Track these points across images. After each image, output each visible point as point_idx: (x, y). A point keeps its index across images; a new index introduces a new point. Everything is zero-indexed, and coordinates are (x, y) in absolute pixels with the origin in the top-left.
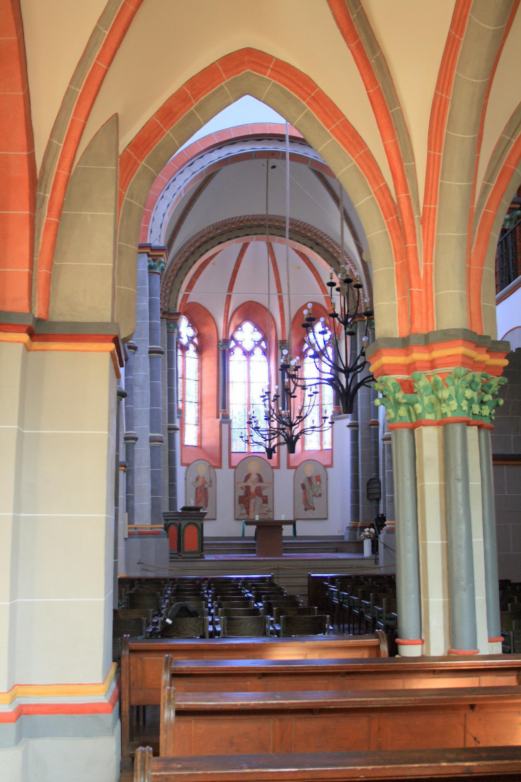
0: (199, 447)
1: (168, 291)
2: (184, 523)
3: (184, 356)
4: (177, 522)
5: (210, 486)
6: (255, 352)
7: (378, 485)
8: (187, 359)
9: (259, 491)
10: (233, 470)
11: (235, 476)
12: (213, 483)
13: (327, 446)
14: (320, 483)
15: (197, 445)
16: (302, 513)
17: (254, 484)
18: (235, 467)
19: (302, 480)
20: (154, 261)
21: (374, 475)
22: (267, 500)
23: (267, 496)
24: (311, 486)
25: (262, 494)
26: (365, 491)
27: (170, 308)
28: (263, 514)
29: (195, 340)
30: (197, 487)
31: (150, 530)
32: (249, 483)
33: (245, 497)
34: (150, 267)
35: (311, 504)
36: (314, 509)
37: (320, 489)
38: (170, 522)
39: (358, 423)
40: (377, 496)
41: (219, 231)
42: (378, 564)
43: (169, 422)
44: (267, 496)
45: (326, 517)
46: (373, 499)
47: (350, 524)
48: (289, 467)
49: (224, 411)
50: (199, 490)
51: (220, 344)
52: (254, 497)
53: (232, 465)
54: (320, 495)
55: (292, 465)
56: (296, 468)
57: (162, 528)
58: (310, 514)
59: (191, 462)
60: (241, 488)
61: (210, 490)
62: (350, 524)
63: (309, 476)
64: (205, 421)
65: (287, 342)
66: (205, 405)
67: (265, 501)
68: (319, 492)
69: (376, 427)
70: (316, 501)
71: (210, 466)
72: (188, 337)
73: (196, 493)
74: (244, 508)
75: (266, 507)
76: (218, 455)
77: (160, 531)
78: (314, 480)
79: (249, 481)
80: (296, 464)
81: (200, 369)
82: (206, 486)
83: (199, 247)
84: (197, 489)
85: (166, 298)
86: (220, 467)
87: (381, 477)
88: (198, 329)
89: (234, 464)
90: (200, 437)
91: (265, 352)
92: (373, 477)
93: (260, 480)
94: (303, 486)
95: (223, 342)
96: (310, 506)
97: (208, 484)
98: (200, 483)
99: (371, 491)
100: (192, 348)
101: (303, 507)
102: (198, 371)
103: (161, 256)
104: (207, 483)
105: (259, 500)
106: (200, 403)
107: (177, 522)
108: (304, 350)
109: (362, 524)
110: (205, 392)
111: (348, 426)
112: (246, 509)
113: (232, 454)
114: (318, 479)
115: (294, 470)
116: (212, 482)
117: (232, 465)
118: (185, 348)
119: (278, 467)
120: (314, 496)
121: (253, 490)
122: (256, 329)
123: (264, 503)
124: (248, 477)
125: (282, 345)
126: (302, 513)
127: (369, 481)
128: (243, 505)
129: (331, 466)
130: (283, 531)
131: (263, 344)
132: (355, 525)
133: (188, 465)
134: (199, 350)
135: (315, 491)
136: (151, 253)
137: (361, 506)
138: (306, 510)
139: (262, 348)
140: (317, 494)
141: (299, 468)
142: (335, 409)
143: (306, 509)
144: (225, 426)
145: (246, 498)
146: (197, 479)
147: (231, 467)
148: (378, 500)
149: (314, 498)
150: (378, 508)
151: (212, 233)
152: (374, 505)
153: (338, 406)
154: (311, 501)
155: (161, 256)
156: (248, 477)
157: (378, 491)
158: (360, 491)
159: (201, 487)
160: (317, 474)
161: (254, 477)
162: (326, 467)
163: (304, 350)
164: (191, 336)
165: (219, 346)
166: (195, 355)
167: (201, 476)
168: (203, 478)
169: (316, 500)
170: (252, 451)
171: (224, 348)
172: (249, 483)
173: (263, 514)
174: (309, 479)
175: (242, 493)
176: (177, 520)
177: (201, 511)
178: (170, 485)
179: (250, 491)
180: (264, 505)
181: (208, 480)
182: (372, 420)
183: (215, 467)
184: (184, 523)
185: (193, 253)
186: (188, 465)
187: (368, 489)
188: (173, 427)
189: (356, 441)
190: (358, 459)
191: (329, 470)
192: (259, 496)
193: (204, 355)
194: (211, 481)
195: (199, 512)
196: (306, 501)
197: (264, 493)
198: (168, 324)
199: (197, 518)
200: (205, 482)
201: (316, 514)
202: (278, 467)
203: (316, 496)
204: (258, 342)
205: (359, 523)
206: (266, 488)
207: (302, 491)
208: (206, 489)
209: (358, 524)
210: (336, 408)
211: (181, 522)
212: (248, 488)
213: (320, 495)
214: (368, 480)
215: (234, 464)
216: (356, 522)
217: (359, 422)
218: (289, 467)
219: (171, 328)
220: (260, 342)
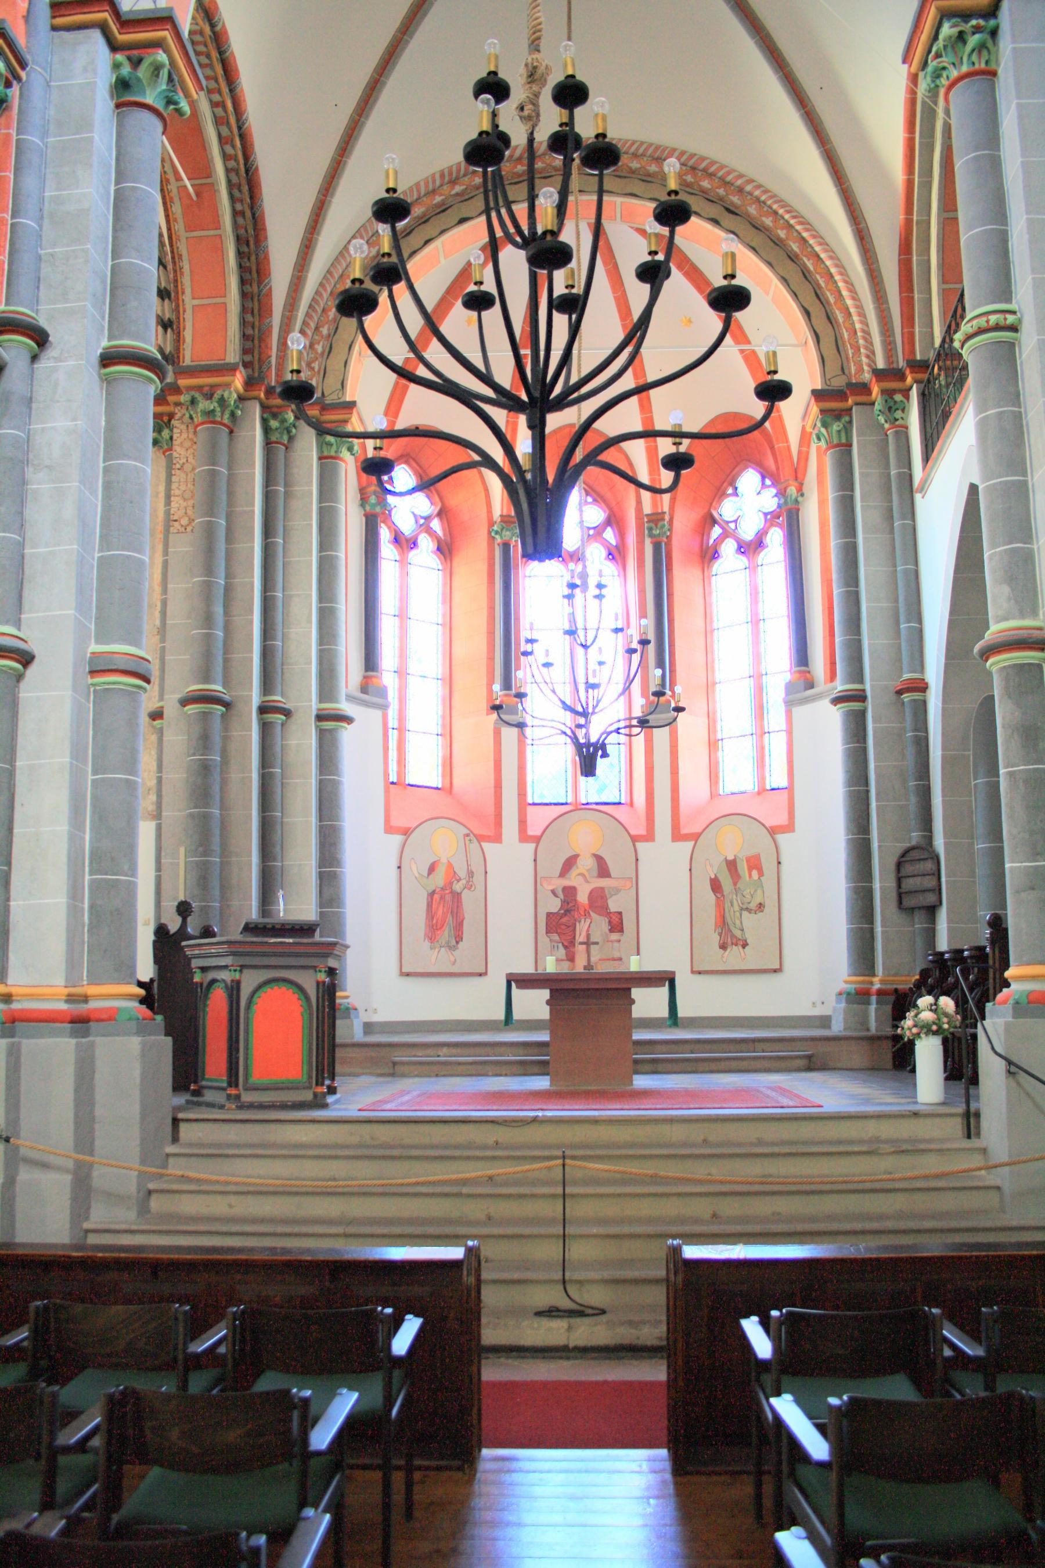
0: (448, 789)
1: (319, 348)
2: (249, 981)
3: (403, 563)
4: (225, 976)
5: (469, 886)
6: (588, 554)
7: (929, 866)
8: (412, 570)
9: (598, 900)
10: (532, 846)
11: (535, 860)
12: (478, 878)
13: (778, 778)
14: (761, 873)
15: (440, 786)
16: (714, 957)
17: (587, 882)
18: (537, 839)
19: (714, 867)
21: (915, 837)
22: (622, 923)
23: (620, 913)
24: (735, 884)
25: (607, 908)
26: (892, 884)
27: (326, 394)
28: (614, 959)
29: (436, 525)
30: (431, 889)
31: (63, 1006)
32: (573, 879)
33: (565, 914)
35: (738, 933)
36: (745, 945)
37: (759, 891)
38: (211, 975)
39: (864, 691)
40: (931, 898)
41: (458, 189)
42: (978, 1134)
43: (322, 699)
44: (620, 913)
45: (778, 967)
46: (919, 908)
47: (846, 982)
48: (677, 836)
49: (506, 695)
50: (436, 896)
51: (495, 528)
52: (587, 914)
53: (530, 833)
54: (761, 906)
55: (684, 831)
56: (695, 837)
57: (131, 997)
58: (734, 957)
59: (414, 826)
60: (554, 892)
61: (466, 896)
62: (846, 982)
63: (730, 857)
65: (667, 517)
66: (458, 685)
67: (617, 925)
68: (758, 899)
69: (916, 696)
70: (750, 925)
71: (468, 835)
72: (415, 515)
73: (429, 905)
74: (560, 945)
75: (619, 941)
76: (491, 810)
77: (116, 1010)
78: (743, 868)
79: (574, 872)
80: (697, 828)
81: (448, 597)
82: (457, 887)
84: (431, 895)
85: (316, 365)
86: (497, 838)
87: (939, 843)
88: (441, 498)
89: (533, 831)
90: (448, 765)
91: (616, 554)
92: (914, 843)
93: (603, 871)
94: (716, 885)
95: (502, 521)
96: (733, 936)
97: (464, 882)
98: (439, 879)
99: (909, 884)
100: (426, 543)
101: (715, 939)
102: (444, 602)
104: (458, 881)
105: (599, 926)
106: (449, 681)
107: (225, 976)
108: (711, 541)
109: (882, 982)
110: (459, 651)
111: (837, 701)
112: (566, 947)
113: (530, 809)
114: (755, 864)
115: (691, 844)
117: (530, 833)
118: (404, 543)
119: (649, 836)
120: (747, 909)
121: (583, 898)
122: (589, 499)
123: (611, 931)
124: (569, 864)
125: (652, 525)
126: (714, 957)
127: (903, 855)
128: (556, 937)
129: (789, 827)
130: (634, 1007)
131: (609, 535)
132: (866, 986)
134: (445, 550)
135: (748, 896)
137: (878, 929)
138: (723, 947)
139: (605, 544)
140: (753, 905)
141: (702, 837)
142: (797, 675)
143: (723, 947)
145: (564, 920)
146: (432, 869)
147: (524, 836)
148: (932, 911)
149: (745, 914)
150: (931, 934)
151: (441, 195)
152: (919, 923)
153: (803, 668)
154: (738, 922)
156: (569, 864)
157: (929, 882)
158: (877, 885)
159: (442, 889)
160: (752, 852)
161: (586, 864)
162: (773, 831)
163: (711, 541)
164: (425, 514)
165: (493, 534)
166: (435, 561)
167: (444, 860)
168: (450, 866)
169: (749, 920)
170: (584, 802)
171: (506, 538)
172: (573, 879)
173: (614, 959)
174: (732, 865)
176: (226, 967)
177: (317, 937)
178: (321, 876)
179: (576, 900)
180: (614, 936)
181: (462, 873)
182: (906, 676)
183: (480, 838)
184: (249, 981)
186: (406, 832)
187: (899, 881)
188: (332, 712)
189: (858, 742)
190: (868, 792)
191: (781, 838)
192: (600, 915)
193: (457, 561)
194: (471, 874)
195: (309, 940)
196: (722, 923)
197: (613, 906)
199: (302, 961)
201: (750, 958)
202: (649, 836)
203: (749, 910)
204: (594, 528)
205: (876, 980)
206: (618, 891)
207: (711, 897)
208: (457, 897)
209: (872, 983)
210: (800, 672)
211: (237, 976)
212: (570, 892)
213: (761, 906)
214: (899, 852)
215: (533, 831)
216: (867, 978)
217: (868, 687)
218: (677, 836)
219: (330, 444)
220: (599, 530)
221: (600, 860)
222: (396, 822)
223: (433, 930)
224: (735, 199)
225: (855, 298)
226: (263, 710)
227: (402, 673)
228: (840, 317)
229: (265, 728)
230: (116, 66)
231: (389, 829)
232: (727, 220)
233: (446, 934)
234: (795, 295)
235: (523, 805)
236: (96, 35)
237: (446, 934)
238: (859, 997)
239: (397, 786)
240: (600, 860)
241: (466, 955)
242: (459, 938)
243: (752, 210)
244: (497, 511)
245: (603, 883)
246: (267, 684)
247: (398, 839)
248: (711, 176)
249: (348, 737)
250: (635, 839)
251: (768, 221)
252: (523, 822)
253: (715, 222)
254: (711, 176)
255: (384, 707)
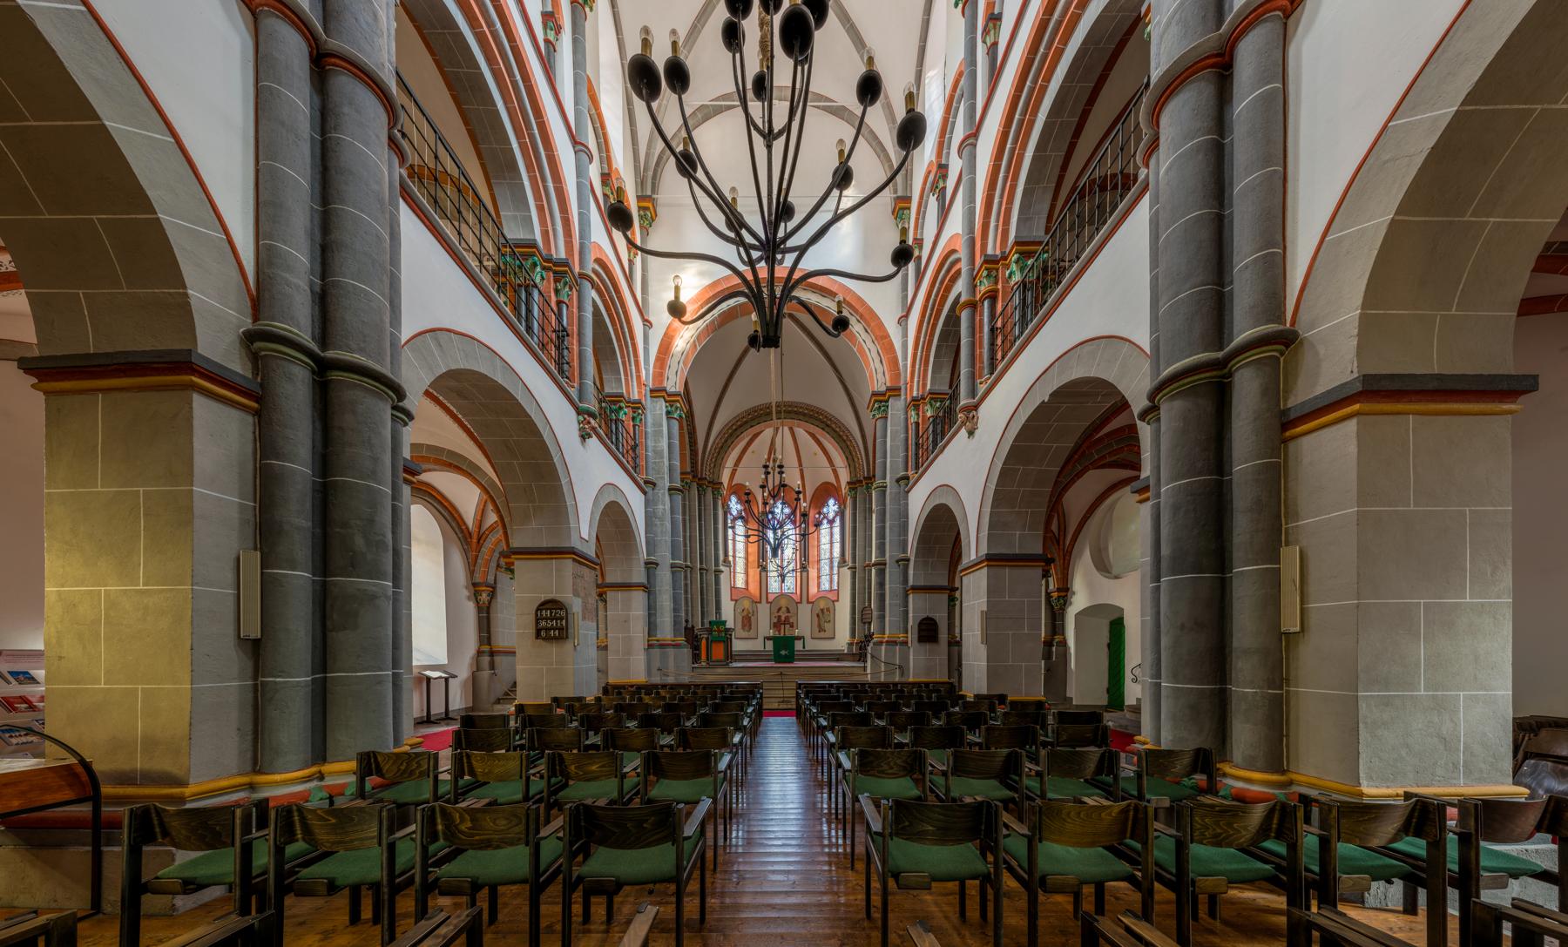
9: (787, 618)
18: (771, 603)
20: (671, 406)
32: (780, 614)
34: (668, 413)
64: (751, 572)
83: (736, 430)
86: (760, 602)
89: (770, 600)
90: (747, 583)
93: (788, 610)
98: (745, 613)
103: (678, 401)
106: (747, 559)
116: (755, 612)
119: (801, 602)
121: (783, 619)
124: (780, 609)
133: (736, 601)
136: (667, 399)
144: (763, 574)
147: (767, 602)
155: (678, 401)
156: (780, 609)
161: (784, 609)
172: (780, 614)
175: (776, 620)
185: (731, 435)
186: (736, 601)
194: (753, 612)
197: (791, 620)
198: (713, 492)
200: (749, 613)
202: (801, 602)
212: (780, 617)
215: (770, 600)
221: (788, 609)
222: (733, 598)
223: (743, 627)
224: (829, 422)
225: (861, 454)
226: (700, 569)
227: (734, 557)
228: (856, 460)
229: (701, 574)
230: (666, 407)
231: (732, 600)
232: (826, 429)
233: (747, 628)
234: (844, 453)
235: (767, 593)
236: (662, 400)
237: (747, 628)
238: (850, 644)
239: (733, 588)
240: (788, 609)
241: (752, 633)
242: (750, 629)
243: (833, 426)
244: (760, 510)
245: (789, 614)
246: (701, 563)
247: (733, 603)
248: (822, 415)
249: (722, 576)
250: (797, 603)
251: (838, 430)
252: (767, 598)
253: (823, 429)
254: (822, 415)
255: (730, 567)
